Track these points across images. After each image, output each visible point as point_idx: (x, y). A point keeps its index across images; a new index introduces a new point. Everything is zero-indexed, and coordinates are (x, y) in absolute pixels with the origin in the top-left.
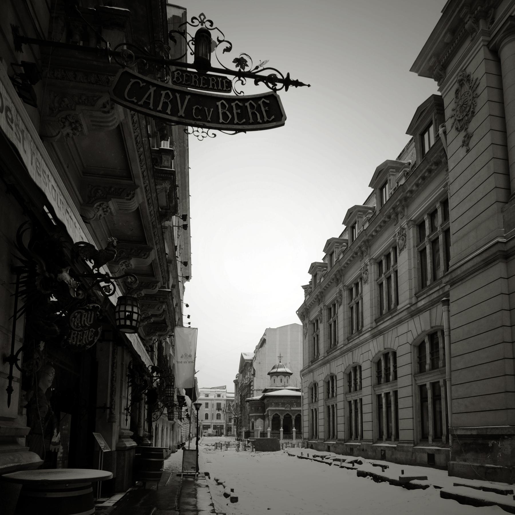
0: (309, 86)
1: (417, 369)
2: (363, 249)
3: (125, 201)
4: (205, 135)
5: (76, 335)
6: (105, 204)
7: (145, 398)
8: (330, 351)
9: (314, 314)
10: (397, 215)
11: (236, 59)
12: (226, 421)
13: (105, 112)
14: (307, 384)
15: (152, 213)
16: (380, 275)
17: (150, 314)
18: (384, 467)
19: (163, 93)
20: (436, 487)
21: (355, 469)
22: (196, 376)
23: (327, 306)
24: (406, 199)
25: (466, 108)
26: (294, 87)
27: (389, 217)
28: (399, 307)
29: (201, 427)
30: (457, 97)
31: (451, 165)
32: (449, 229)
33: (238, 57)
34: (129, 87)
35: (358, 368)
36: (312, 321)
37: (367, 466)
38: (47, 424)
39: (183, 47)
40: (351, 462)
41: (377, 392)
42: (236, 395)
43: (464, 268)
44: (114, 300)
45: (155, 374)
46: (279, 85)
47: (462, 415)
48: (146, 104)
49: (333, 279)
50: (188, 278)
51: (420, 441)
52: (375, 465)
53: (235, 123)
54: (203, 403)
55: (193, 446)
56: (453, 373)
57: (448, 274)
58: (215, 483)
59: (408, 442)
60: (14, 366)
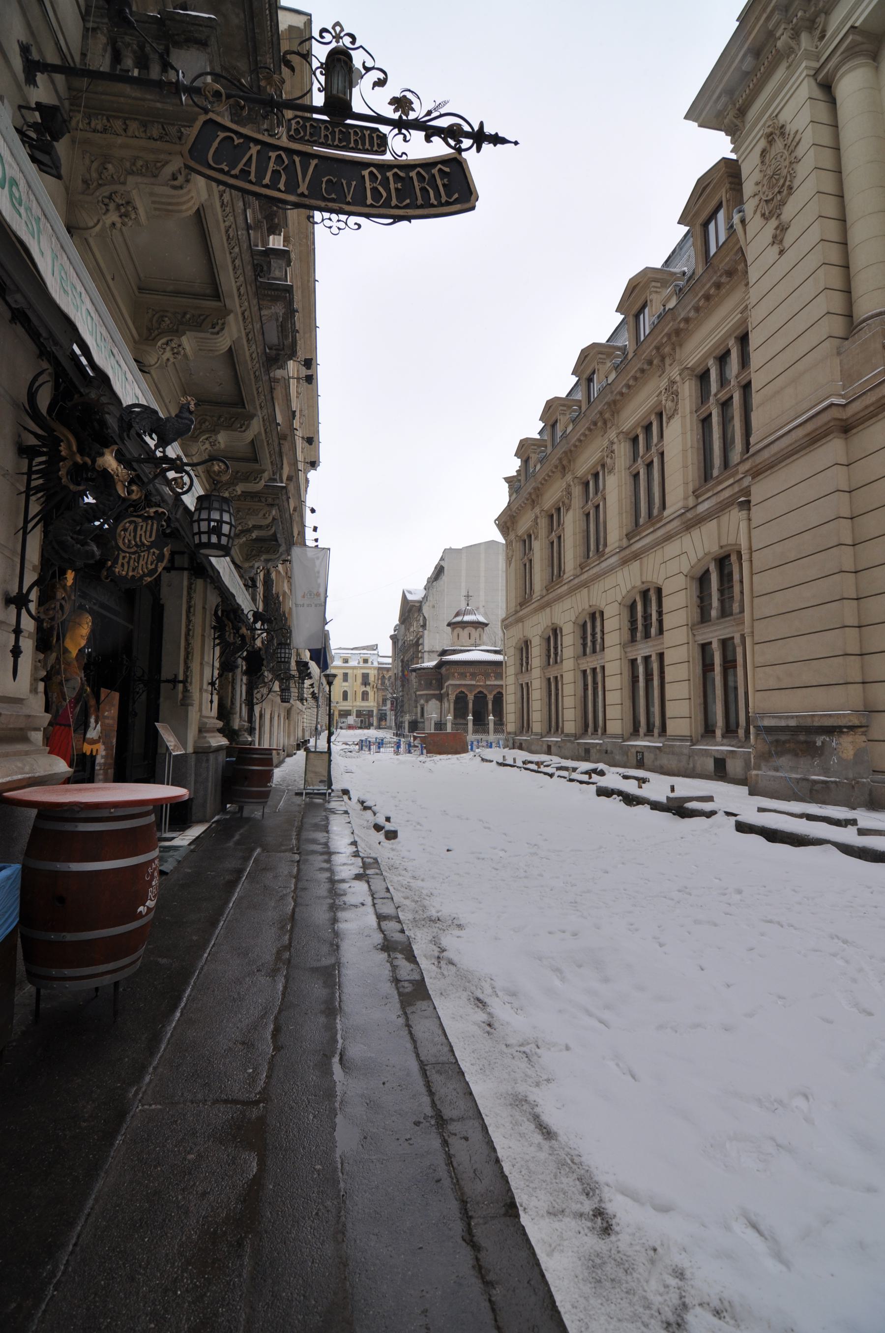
0: (516, 143)
1: (696, 616)
2: (607, 415)
3: (208, 335)
4: (342, 225)
5: (126, 560)
6: (176, 340)
7: (242, 664)
8: (552, 587)
9: (524, 525)
10: (663, 359)
11: (394, 98)
12: (378, 704)
13: (175, 188)
14: (513, 642)
15: (254, 356)
16: (635, 460)
17: (251, 524)
18: (642, 781)
19: (273, 155)
20: (728, 814)
21: (593, 783)
22: (327, 627)
23: (546, 511)
24: (678, 332)
25: (778, 180)
26: (492, 145)
27: (650, 363)
28: (666, 513)
29: (336, 713)
30: (762, 162)
31: (753, 274)
32: (749, 383)
33: (398, 95)
34: (215, 145)
35: (597, 615)
36: (520, 537)
37: (613, 779)
38: (78, 709)
39: (306, 80)
40: (586, 773)
41: (629, 654)
42: (394, 660)
43: (775, 448)
44: (190, 501)
45: (258, 625)
46: (466, 143)
47: (773, 692)
48: (244, 174)
49: (556, 467)
50: (314, 464)
51: (702, 736)
52: (626, 777)
53: (393, 205)
54: (339, 673)
55: (322, 745)
56: (756, 623)
57: (747, 459)
58: (359, 806)
59: (682, 739)
60: (24, 611)
